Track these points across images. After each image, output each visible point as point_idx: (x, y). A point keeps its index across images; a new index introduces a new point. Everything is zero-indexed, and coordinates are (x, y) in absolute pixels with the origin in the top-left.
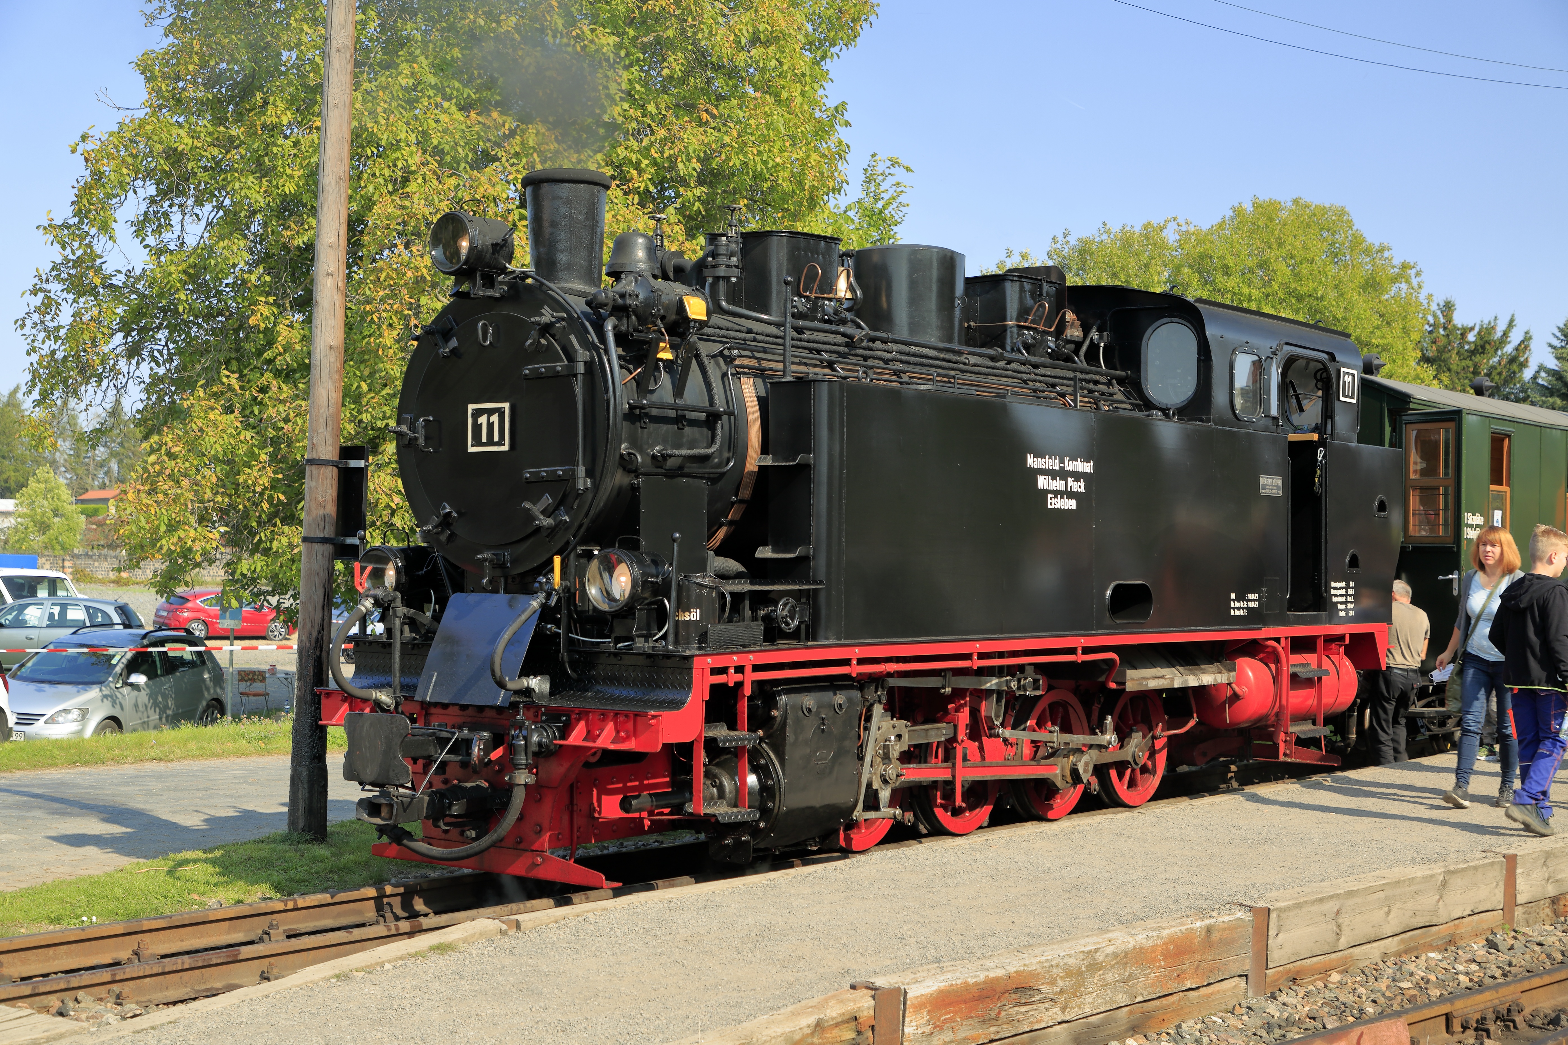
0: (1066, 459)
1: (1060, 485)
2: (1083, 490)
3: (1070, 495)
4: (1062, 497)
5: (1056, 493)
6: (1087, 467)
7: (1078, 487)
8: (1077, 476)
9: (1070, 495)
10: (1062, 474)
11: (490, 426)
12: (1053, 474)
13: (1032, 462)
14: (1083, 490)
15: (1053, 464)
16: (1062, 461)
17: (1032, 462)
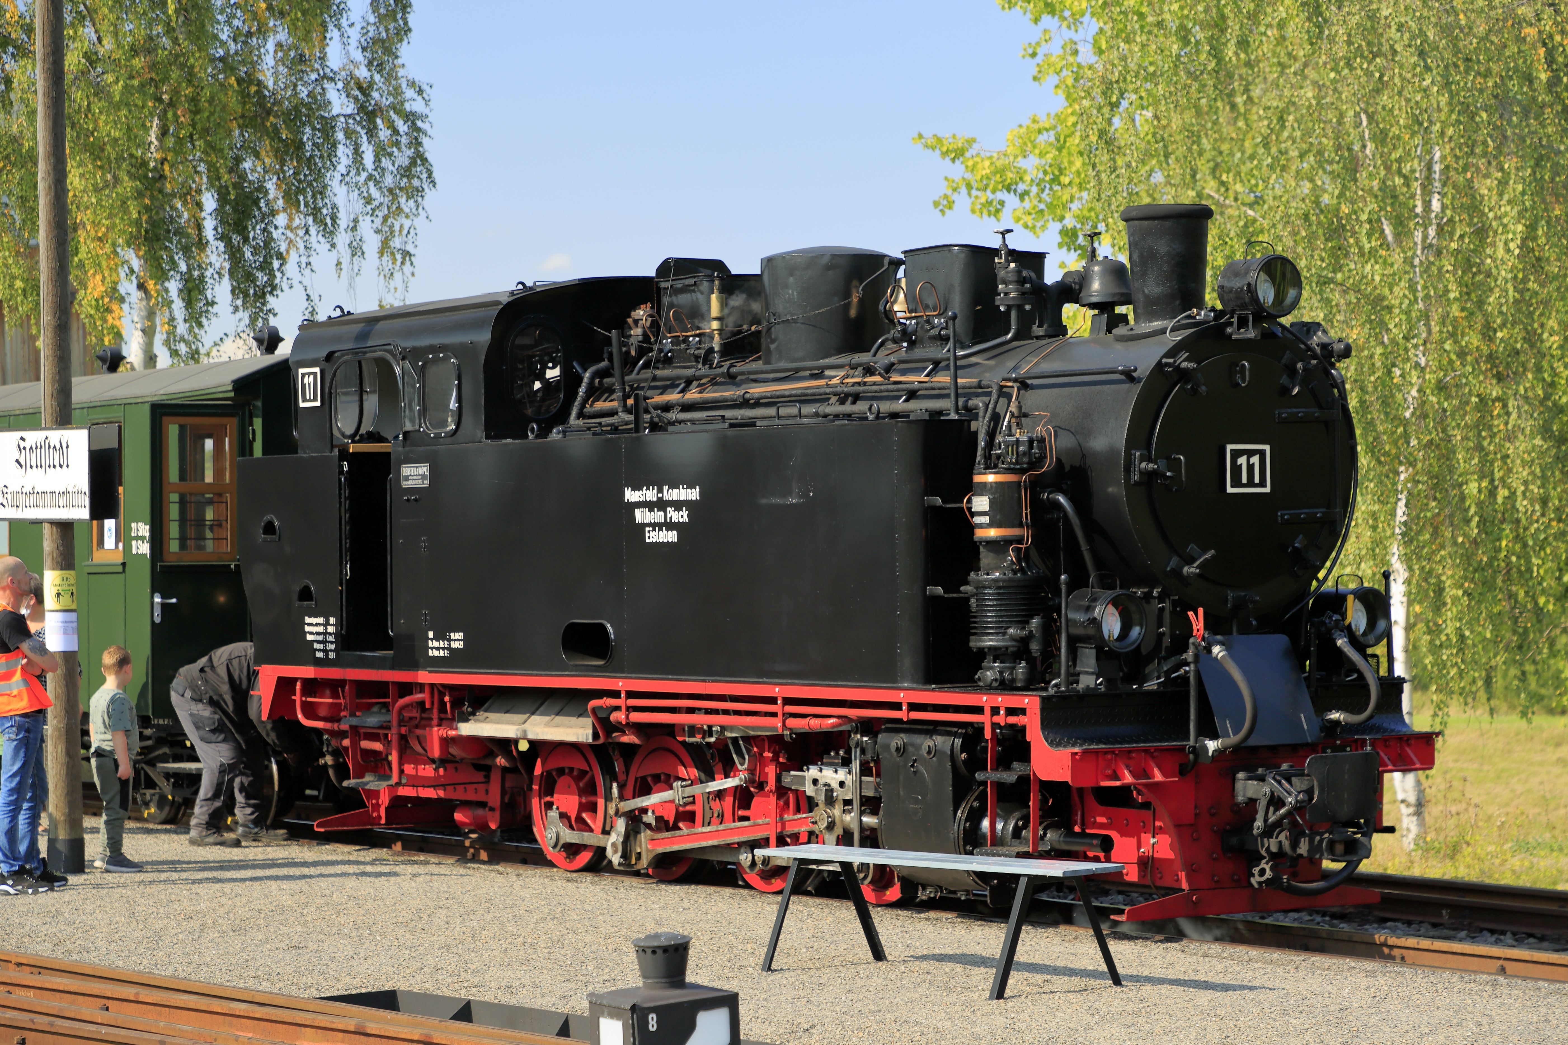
0: (665, 488)
1: (657, 516)
2: (686, 519)
3: (669, 525)
4: (661, 529)
5: (654, 526)
6: (693, 494)
7: (681, 516)
8: (678, 505)
9: (669, 525)
10: (661, 505)
12: (650, 506)
13: (631, 496)
14: (686, 519)
15: (651, 495)
16: (660, 491)
17: (631, 496)
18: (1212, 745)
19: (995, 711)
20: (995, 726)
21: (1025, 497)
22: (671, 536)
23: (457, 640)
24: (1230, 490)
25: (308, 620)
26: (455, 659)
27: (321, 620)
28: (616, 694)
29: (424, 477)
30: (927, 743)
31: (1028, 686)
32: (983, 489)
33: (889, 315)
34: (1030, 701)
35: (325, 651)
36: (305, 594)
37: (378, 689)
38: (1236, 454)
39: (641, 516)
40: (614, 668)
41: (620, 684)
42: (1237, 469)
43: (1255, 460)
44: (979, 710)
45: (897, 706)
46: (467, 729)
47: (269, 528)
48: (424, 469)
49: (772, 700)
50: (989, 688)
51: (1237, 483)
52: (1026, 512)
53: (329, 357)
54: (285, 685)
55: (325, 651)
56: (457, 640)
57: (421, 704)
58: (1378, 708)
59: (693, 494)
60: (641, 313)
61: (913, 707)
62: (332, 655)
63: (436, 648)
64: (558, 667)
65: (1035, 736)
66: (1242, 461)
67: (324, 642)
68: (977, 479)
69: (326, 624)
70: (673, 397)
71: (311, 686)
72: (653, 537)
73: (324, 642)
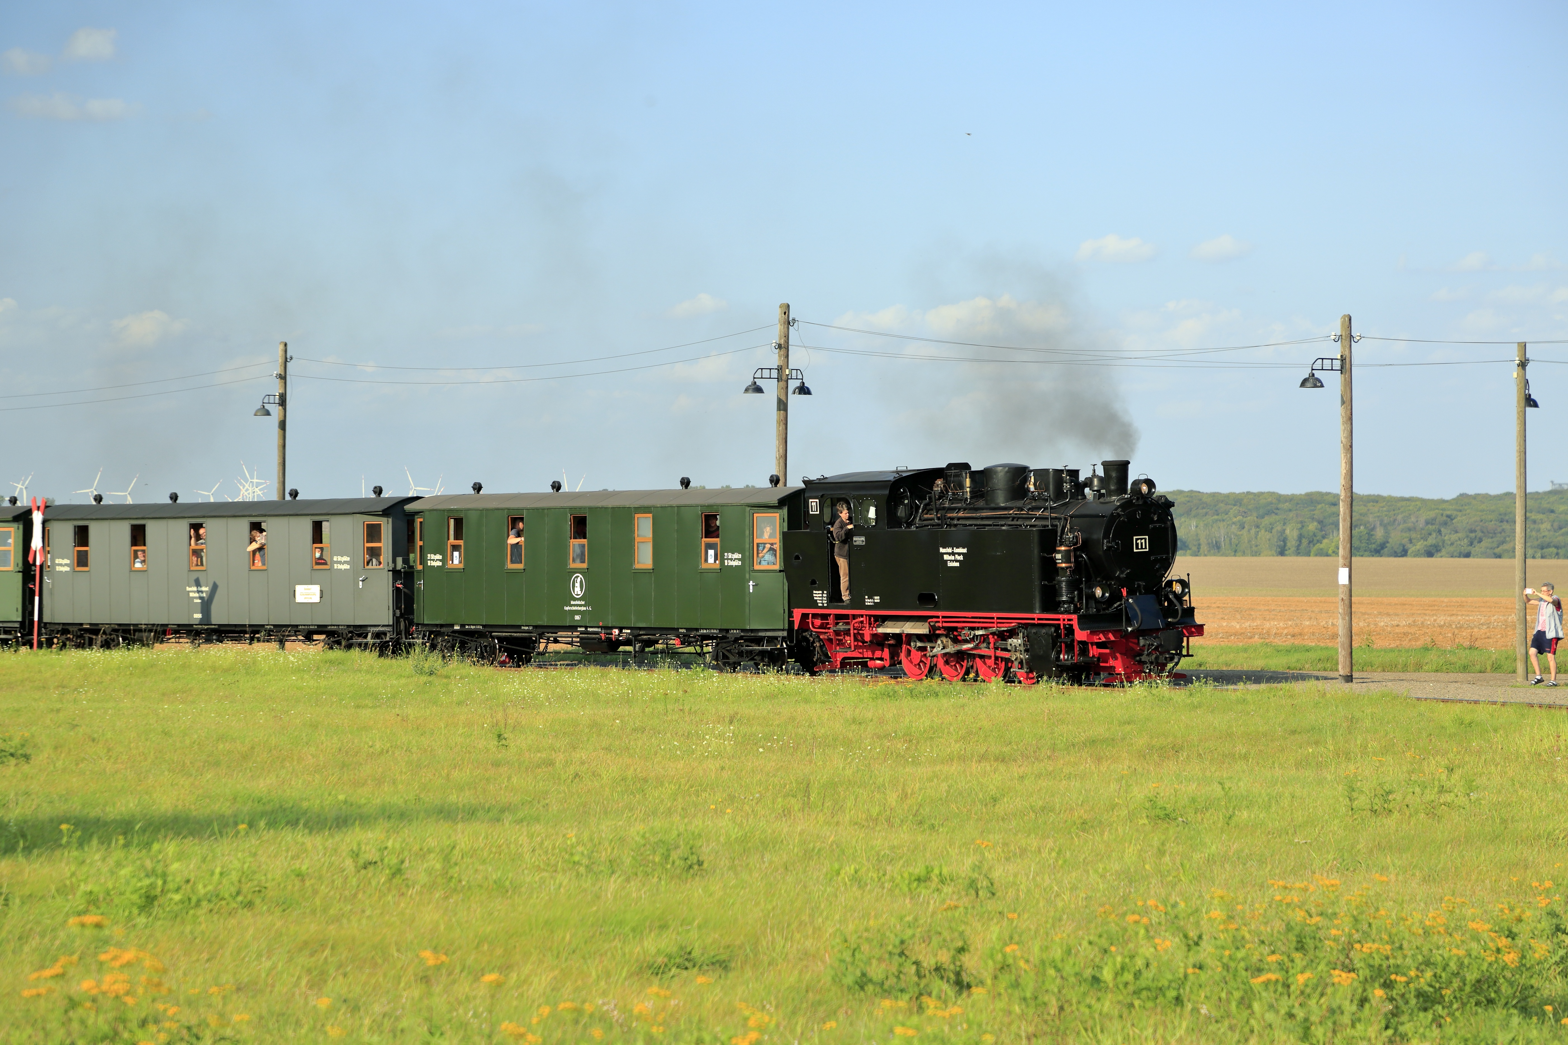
3: (957, 561)
5: (951, 561)
6: (965, 551)
7: (961, 558)
8: (959, 554)
9: (957, 561)
10: (953, 554)
12: (949, 554)
13: (942, 550)
15: (949, 550)
17: (942, 550)
18: (1130, 629)
19: (1064, 620)
20: (1064, 625)
21: (1072, 554)
22: (957, 564)
23: (877, 599)
24: (1135, 550)
26: (876, 606)
28: (938, 617)
30: (1044, 631)
31: (1075, 612)
32: (1059, 552)
33: (1028, 489)
34: (1074, 617)
37: (846, 617)
38: (1137, 540)
39: (946, 557)
40: (937, 607)
41: (940, 614)
42: (1137, 544)
43: (1143, 541)
44: (1059, 620)
45: (1034, 619)
46: (881, 630)
47: (797, 558)
48: (863, 539)
49: (993, 618)
50: (1062, 613)
51: (1137, 548)
52: (1073, 560)
53: (822, 496)
54: (805, 616)
56: (877, 599)
57: (862, 622)
58: (1182, 617)
59: (965, 551)
60: (939, 482)
61: (1039, 619)
63: (869, 602)
64: (917, 609)
65: (1076, 627)
66: (1139, 541)
68: (1058, 548)
70: (955, 515)
71: (815, 616)
72: (950, 564)
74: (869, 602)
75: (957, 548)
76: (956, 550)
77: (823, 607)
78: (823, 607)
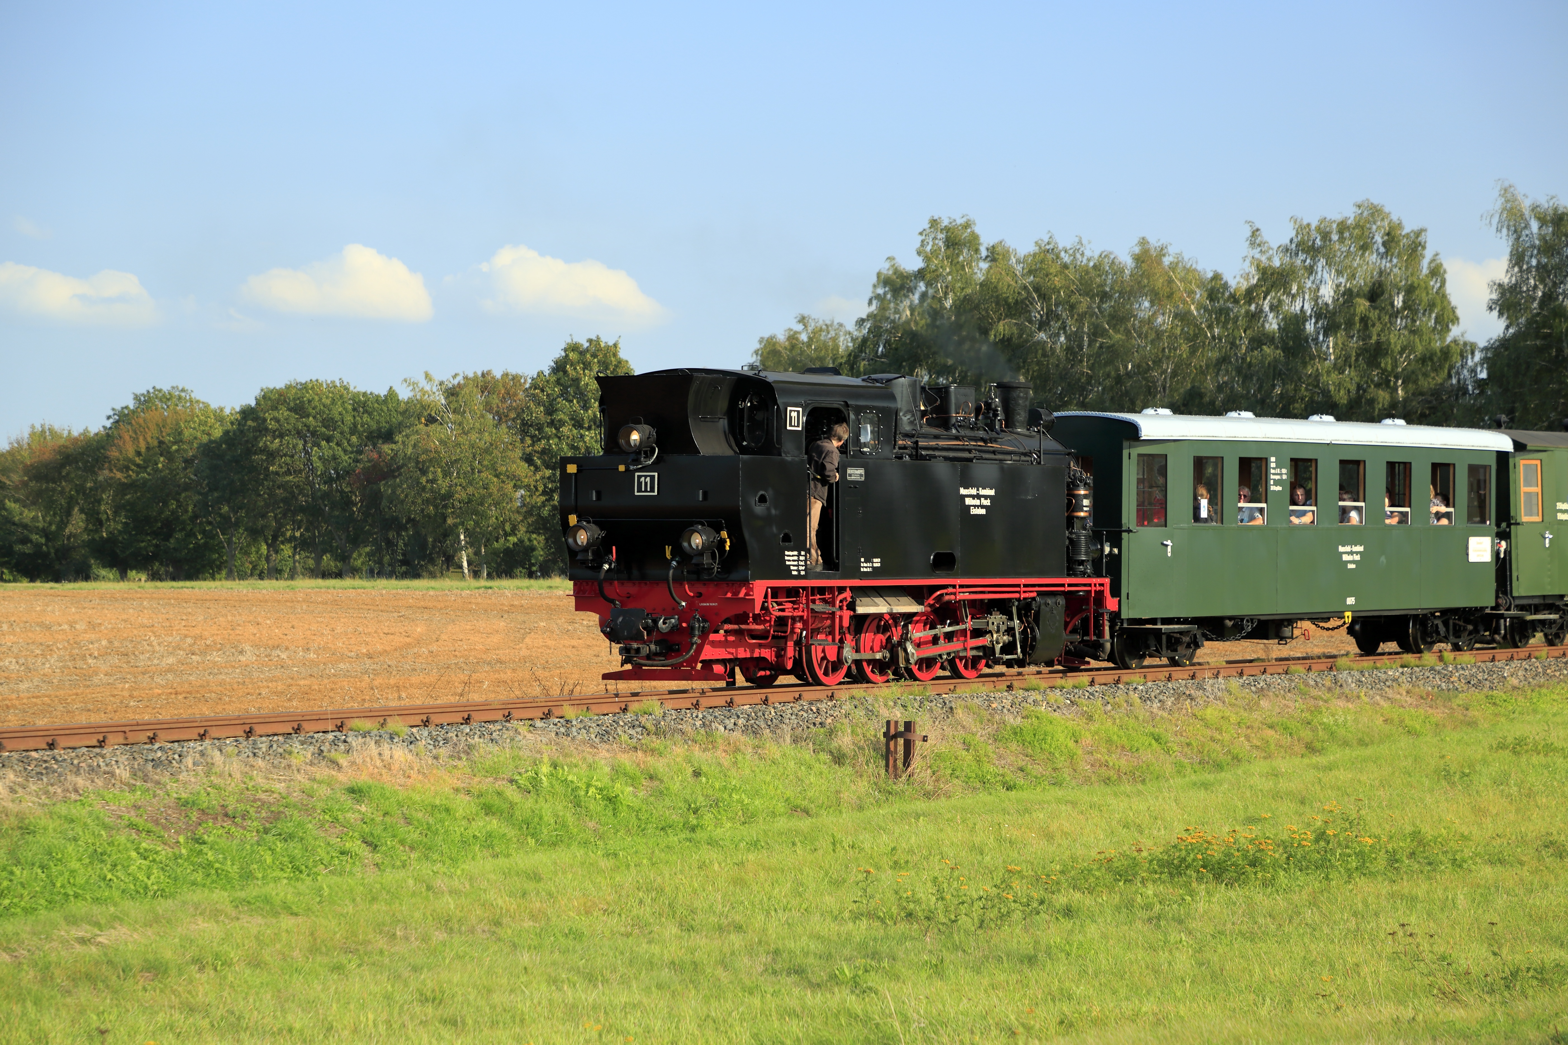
3: (982, 507)
5: (975, 506)
6: (992, 492)
8: (986, 497)
10: (978, 497)
11: (646, 483)
12: (973, 497)
15: (973, 491)
22: (983, 512)
25: (787, 553)
27: (796, 553)
29: (861, 475)
35: (798, 571)
36: (786, 538)
44: (1090, 585)
45: (1063, 585)
49: (1019, 586)
55: (798, 571)
56: (877, 562)
59: (992, 492)
62: (803, 573)
63: (865, 567)
67: (798, 566)
69: (799, 555)
73: (798, 566)
74: (865, 567)
75: (984, 488)
76: (983, 492)
77: (799, 577)
78: (799, 577)
